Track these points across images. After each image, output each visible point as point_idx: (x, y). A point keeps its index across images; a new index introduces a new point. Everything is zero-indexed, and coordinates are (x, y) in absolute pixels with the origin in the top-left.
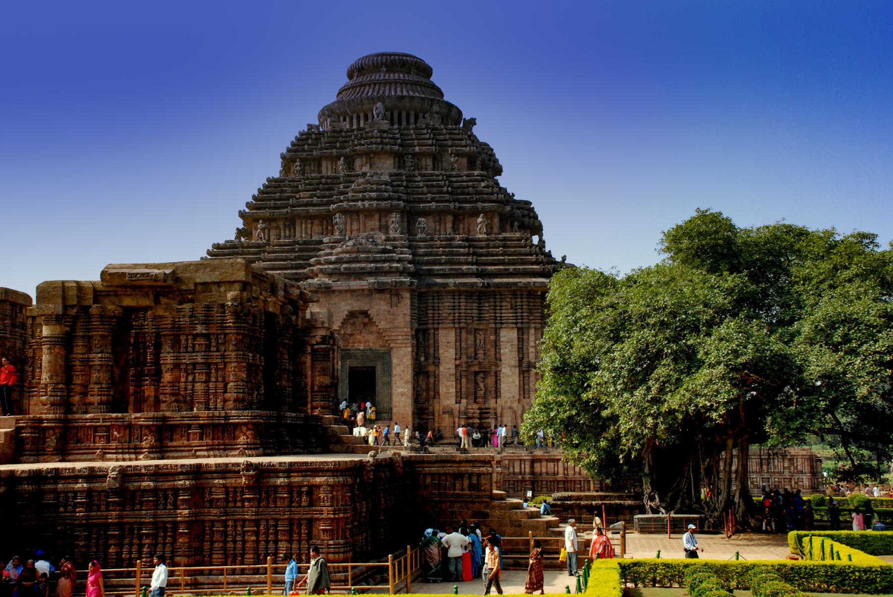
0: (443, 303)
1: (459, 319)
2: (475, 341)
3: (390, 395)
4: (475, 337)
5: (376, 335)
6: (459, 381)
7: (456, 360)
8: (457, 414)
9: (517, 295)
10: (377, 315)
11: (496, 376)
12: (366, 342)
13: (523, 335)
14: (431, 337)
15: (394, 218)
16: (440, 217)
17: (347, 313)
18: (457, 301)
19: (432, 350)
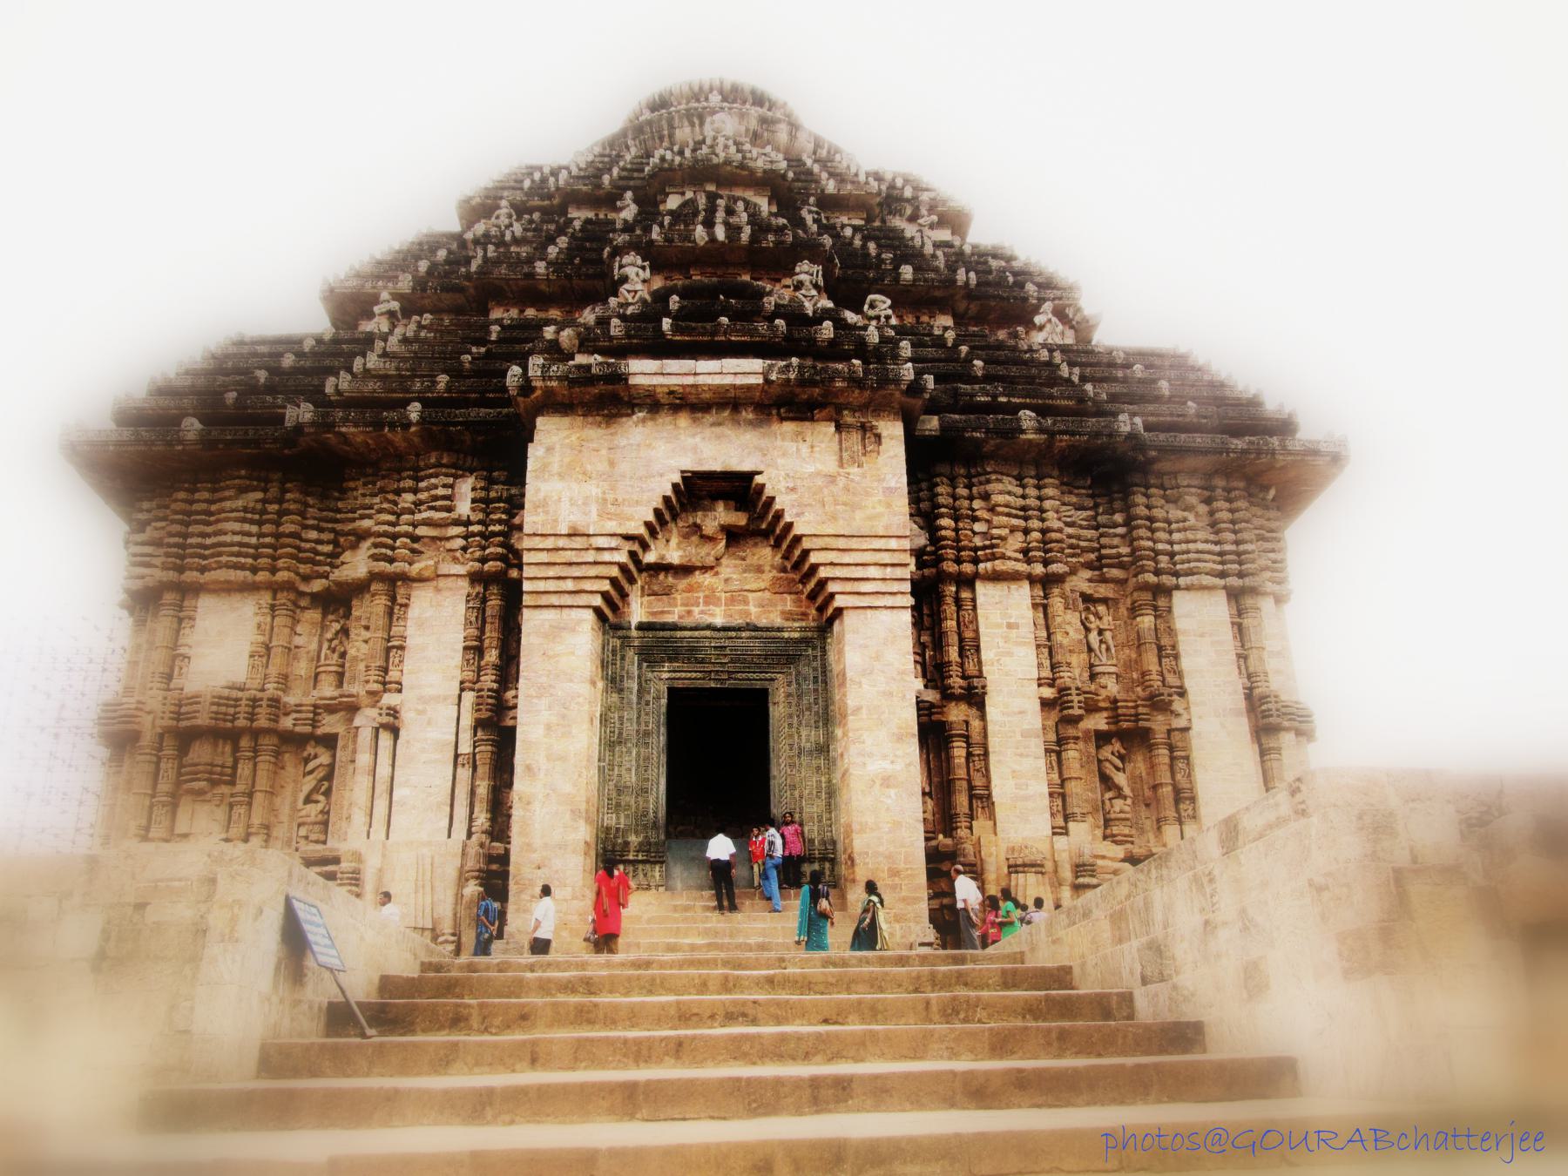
0: (986, 497)
1: (1046, 552)
2: (1088, 630)
3: (831, 794)
4: (1083, 624)
5: (770, 575)
6: (1054, 757)
7: (1040, 685)
8: (1067, 874)
9: (1211, 488)
10: (793, 489)
11: (1171, 748)
12: (732, 601)
13: (1240, 614)
14: (950, 609)
15: (807, 271)
16: (918, 318)
17: (677, 478)
18: (1032, 492)
19: (953, 654)
